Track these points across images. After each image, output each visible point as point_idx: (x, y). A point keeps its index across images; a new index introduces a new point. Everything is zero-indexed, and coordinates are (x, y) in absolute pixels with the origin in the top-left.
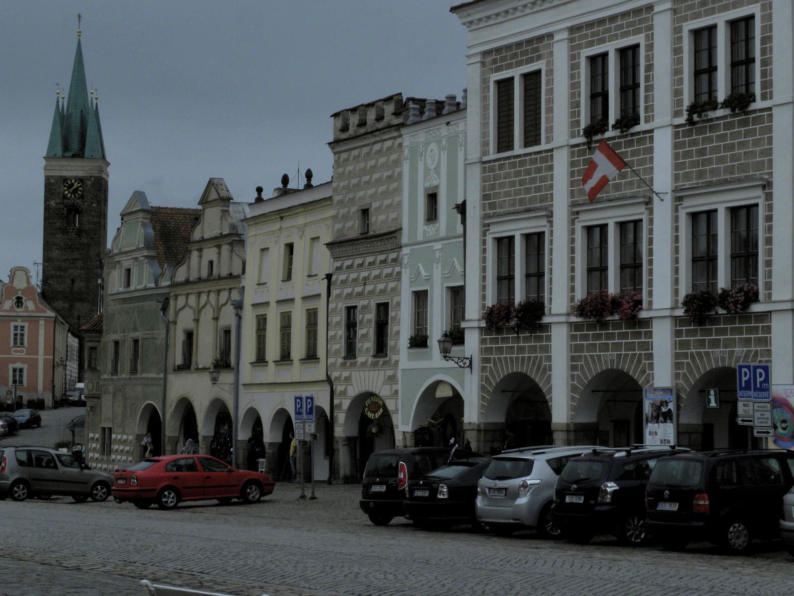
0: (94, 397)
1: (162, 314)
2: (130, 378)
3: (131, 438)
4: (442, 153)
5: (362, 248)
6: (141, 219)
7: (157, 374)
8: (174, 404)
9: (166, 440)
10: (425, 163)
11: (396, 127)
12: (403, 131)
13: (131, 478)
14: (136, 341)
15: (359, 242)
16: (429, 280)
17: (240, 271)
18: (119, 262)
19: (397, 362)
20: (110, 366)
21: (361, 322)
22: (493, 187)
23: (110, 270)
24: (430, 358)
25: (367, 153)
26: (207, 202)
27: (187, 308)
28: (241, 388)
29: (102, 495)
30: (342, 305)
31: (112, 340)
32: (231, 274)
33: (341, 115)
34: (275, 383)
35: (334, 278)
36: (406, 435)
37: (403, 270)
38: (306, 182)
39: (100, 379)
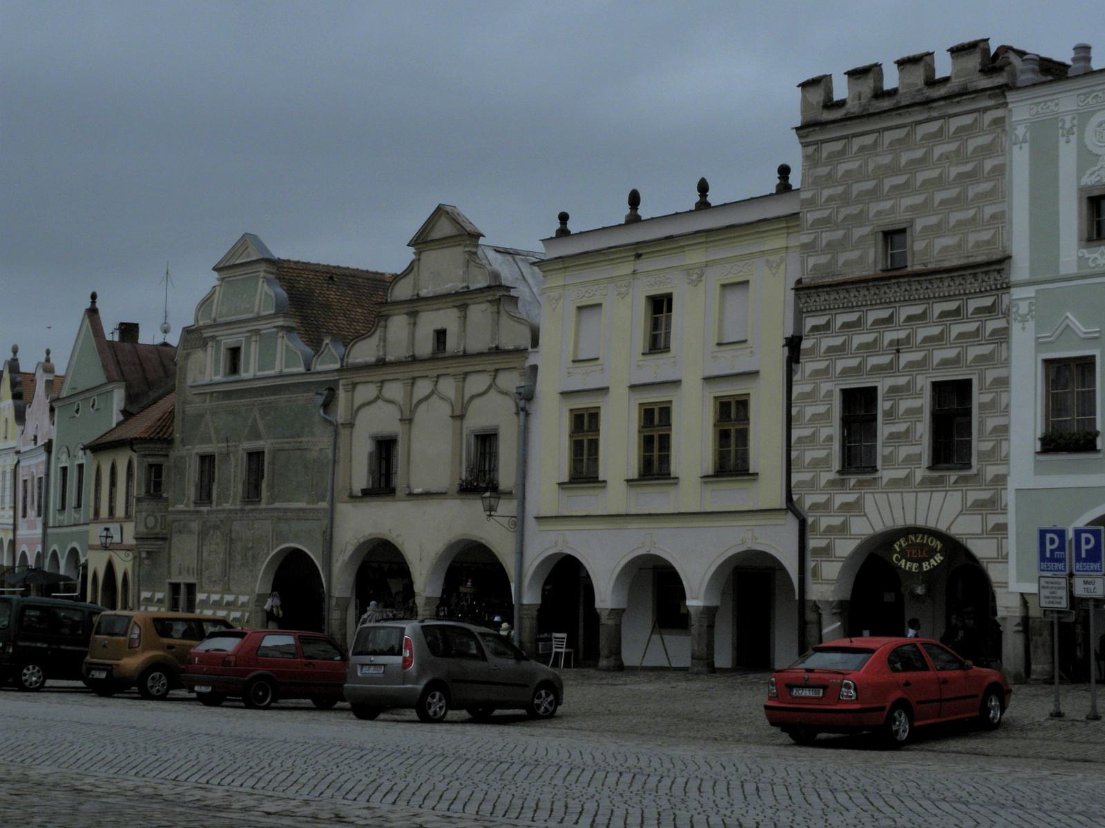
0: (157, 538)
1: (322, 412)
2: (242, 510)
3: (243, 599)
5: (891, 293)
6: (262, 274)
7: (308, 503)
8: (350, 550)
9: (334, 602)
10: (1082, 147)
11: (998, 91)
12: (1011, 97)
13: (841, 685)
14: (255, 457)
15: (893, 281)
17: (525, 342)
18: (213, 338)
19: (1001, 480)
20: (192, 492)
21: (889, 414)
23: (190, 351)
25: (899, 141)
26: (425, 242)
27: (380, 403)
28: (530, 524)
29: (548, 706)
30: (832, 388)
31: (197, 454)
32: (497, 348)
33: (823, 83)
34: (627, 515)
35: (806, 344)
36: (1028, 599)
37: (1016, 328)
38: (698, 199)
39: (167, 511)
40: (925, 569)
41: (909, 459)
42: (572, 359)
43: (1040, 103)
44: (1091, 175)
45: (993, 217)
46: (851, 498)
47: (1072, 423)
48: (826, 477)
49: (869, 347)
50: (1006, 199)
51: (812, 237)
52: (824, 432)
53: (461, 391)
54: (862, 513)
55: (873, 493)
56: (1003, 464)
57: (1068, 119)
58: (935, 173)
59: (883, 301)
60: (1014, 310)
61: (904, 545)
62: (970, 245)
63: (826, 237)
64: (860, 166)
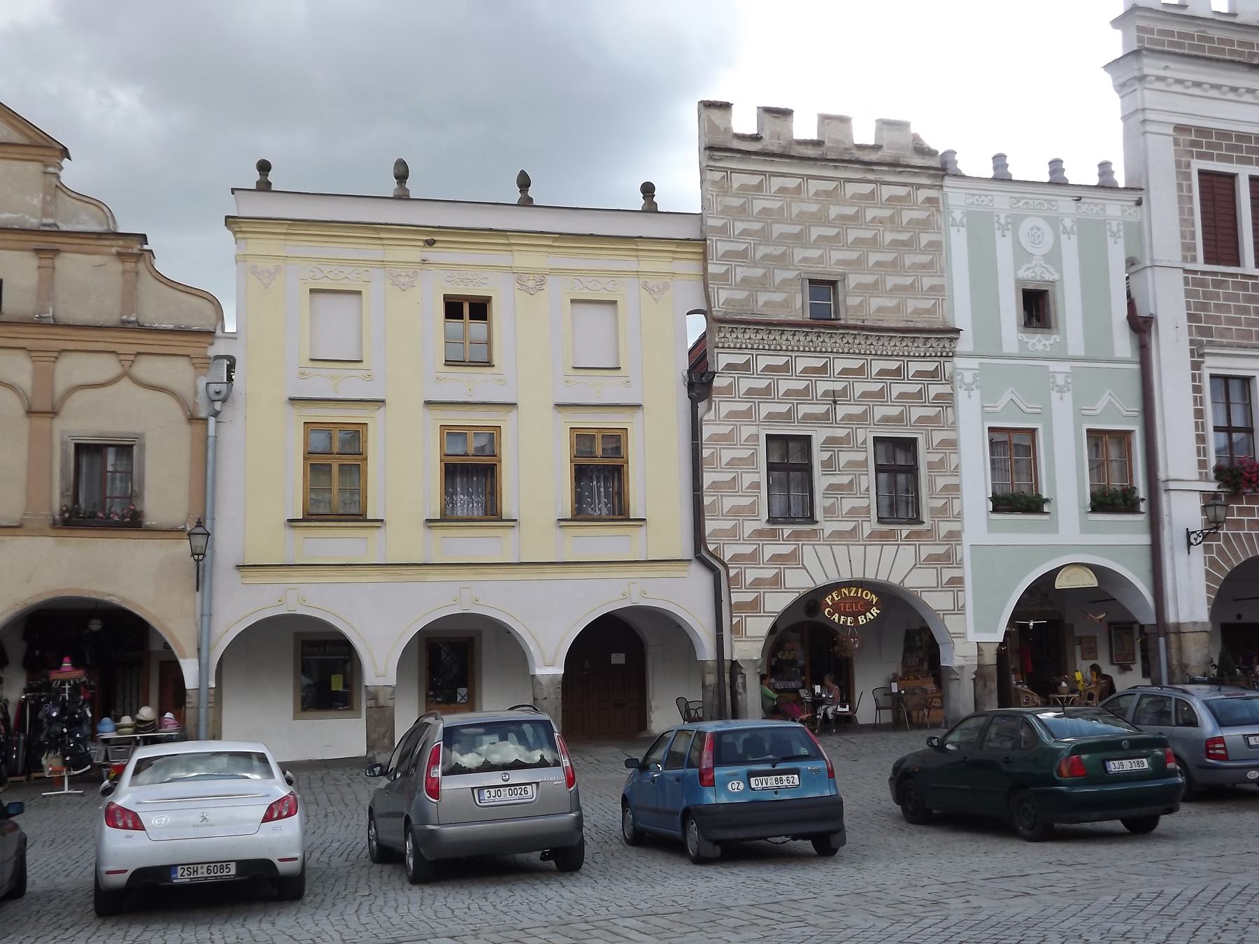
4: (1064, 237)
12: (948, 181)
16: (1045, 413)
19: (954, 536)
21: (828, 465)
22: (1204, 307)
24: (1055, 530)
25: (827, 193)
37: (961, 395)
40: (861, 623)
41: (853, 511)
42: (309, 356)
43: (975, 195)
44: (1027, 270)
45: (932, 288)
46: (786, 549)
47: (1023, 485)
48: (750, 527)
49: (803, 395)
50: (945, 274)
51: (725, 268)
52: (748, 479)
53: (44, 378)
54: (801, 566)
55: (813, 545)
56: (956, 521)
57: (1002, 216)
58: (869, 234)
59: (818, 349)
60: (959, 378)
61: (836, 599)
62: (909, 311)
63: (741, 272)
64: (782, 208)
